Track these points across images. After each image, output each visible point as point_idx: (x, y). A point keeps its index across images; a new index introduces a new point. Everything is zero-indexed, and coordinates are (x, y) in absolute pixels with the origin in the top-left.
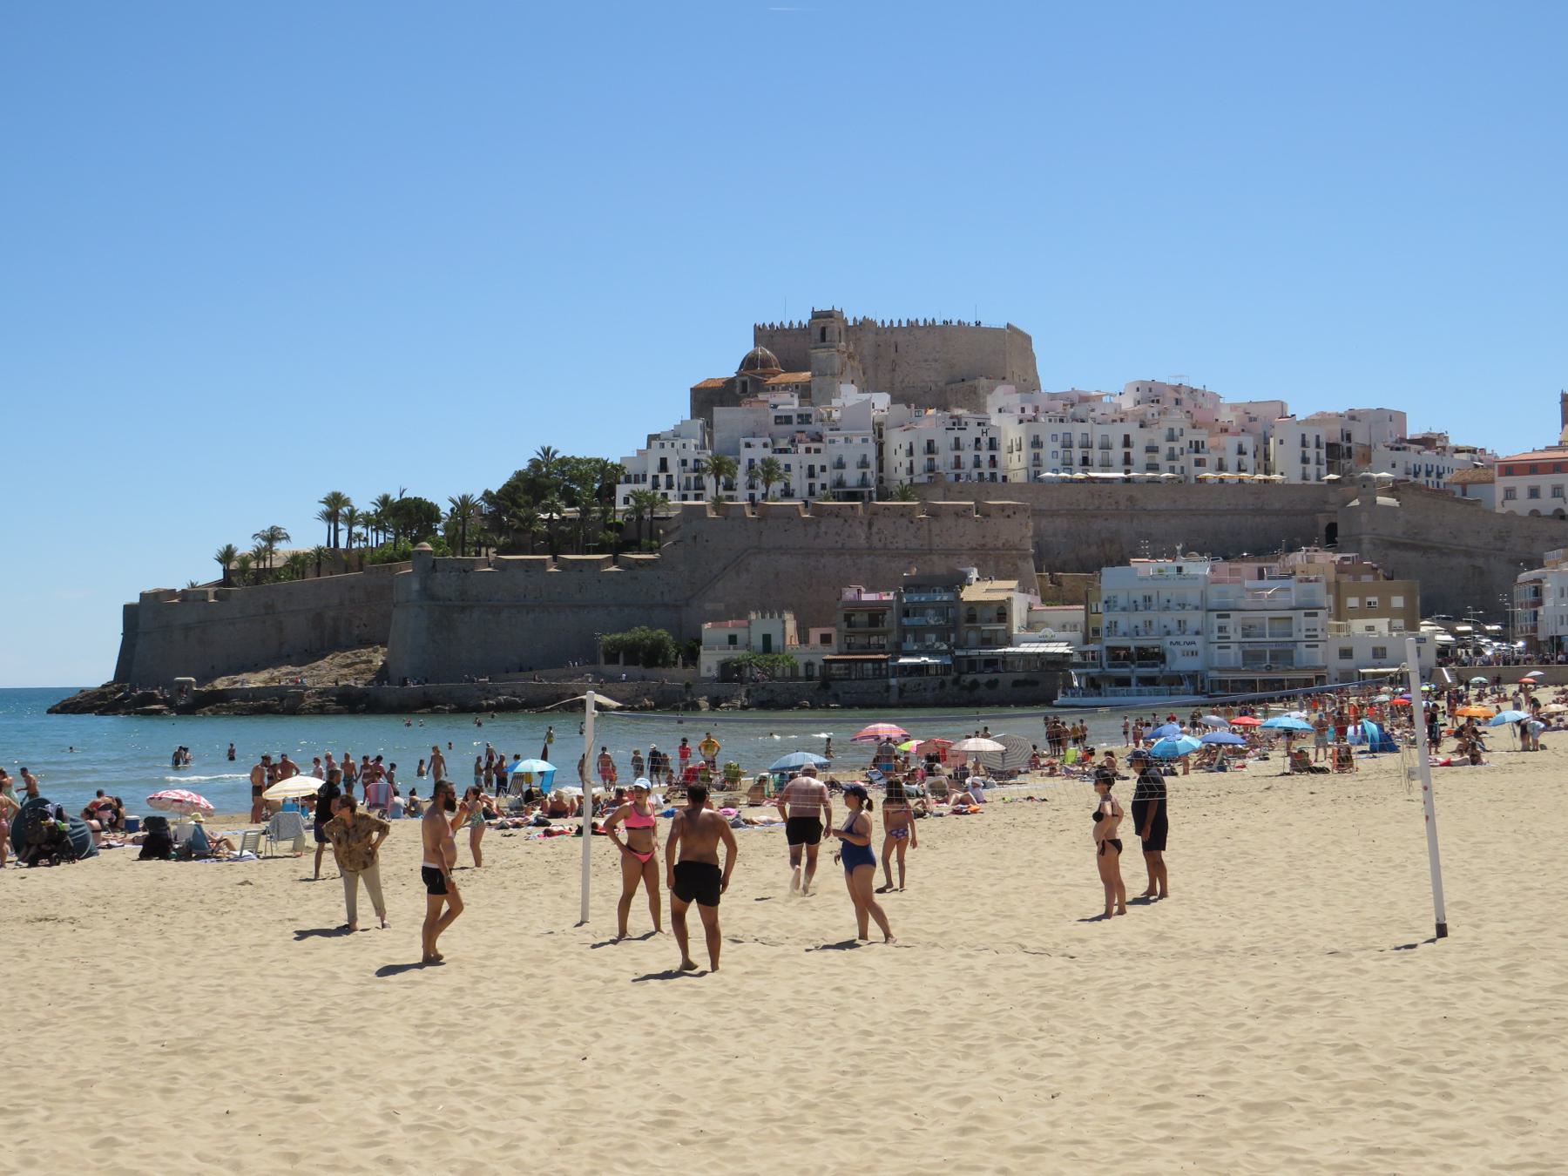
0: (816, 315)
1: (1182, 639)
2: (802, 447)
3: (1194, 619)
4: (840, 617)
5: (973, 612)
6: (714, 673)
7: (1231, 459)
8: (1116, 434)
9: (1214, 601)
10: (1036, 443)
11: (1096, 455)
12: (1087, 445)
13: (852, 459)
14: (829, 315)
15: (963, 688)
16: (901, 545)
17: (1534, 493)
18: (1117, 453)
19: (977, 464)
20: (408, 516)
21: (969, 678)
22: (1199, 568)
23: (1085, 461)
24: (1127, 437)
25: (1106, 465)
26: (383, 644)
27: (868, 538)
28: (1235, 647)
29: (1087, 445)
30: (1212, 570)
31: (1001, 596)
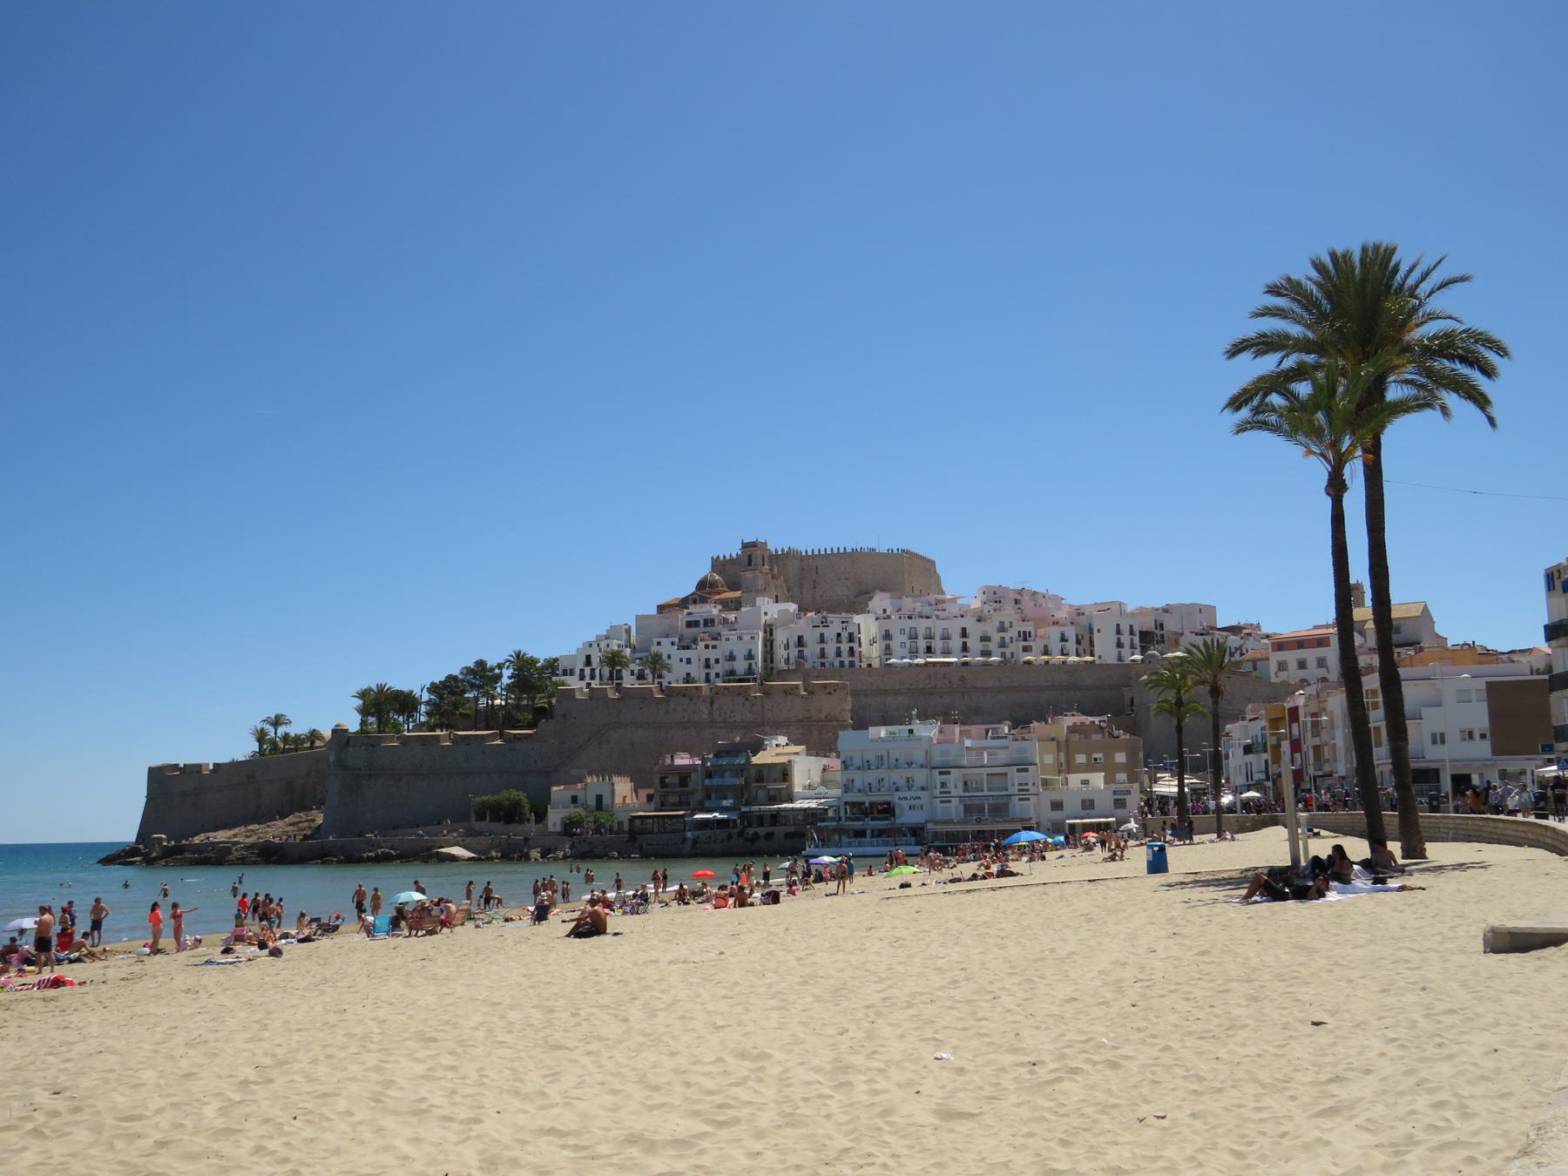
0: (745, 546)
1: (909, 794)
2: (702, 644)
3: (920, 776)
4: (657, 780)
5: (763, 772)
6: (558, 828)
7: (1055, 645)
8: (955, 628)
9: (937, 759)
10: (887, 636)
11: (938, 644)
12: (930, 637)
13: (740, 653)
14: (754, 545)
15: (747, 840)
17: (1302, 665)
18: (956, 643)
19: (839, 654)
20: (383, 704)
21: (751, 831)
22: (928, 731)
23: (929, 650)
24: (964, 630)
25: (947, 653)
26: (320, 804)
27: (710, 713)
28: (955, 801)
29: (930, 637)
30: (941, 732)
31: (783, 759)
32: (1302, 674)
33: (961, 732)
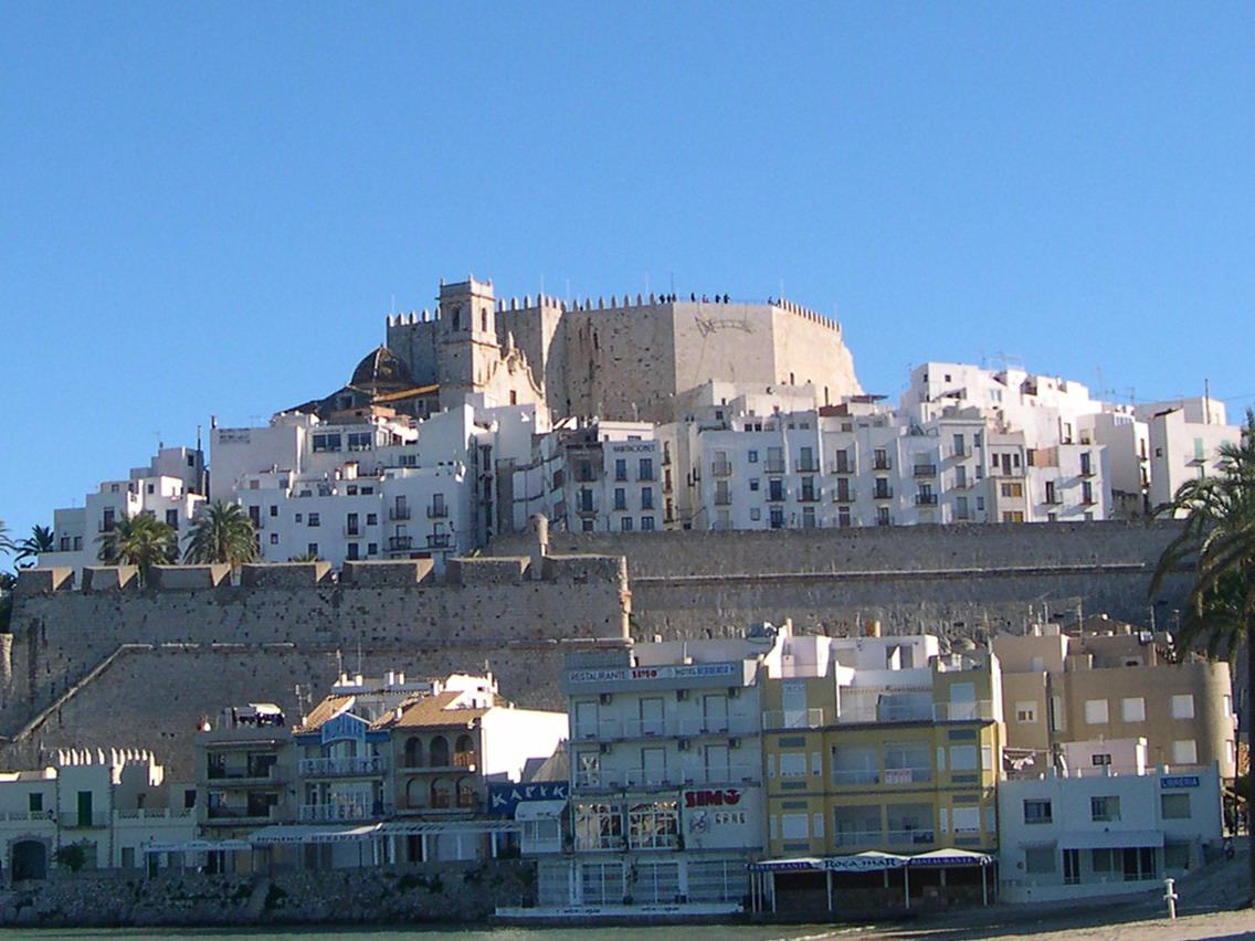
16: (391, 632)
19: (620, 504)
33: (832, 651)
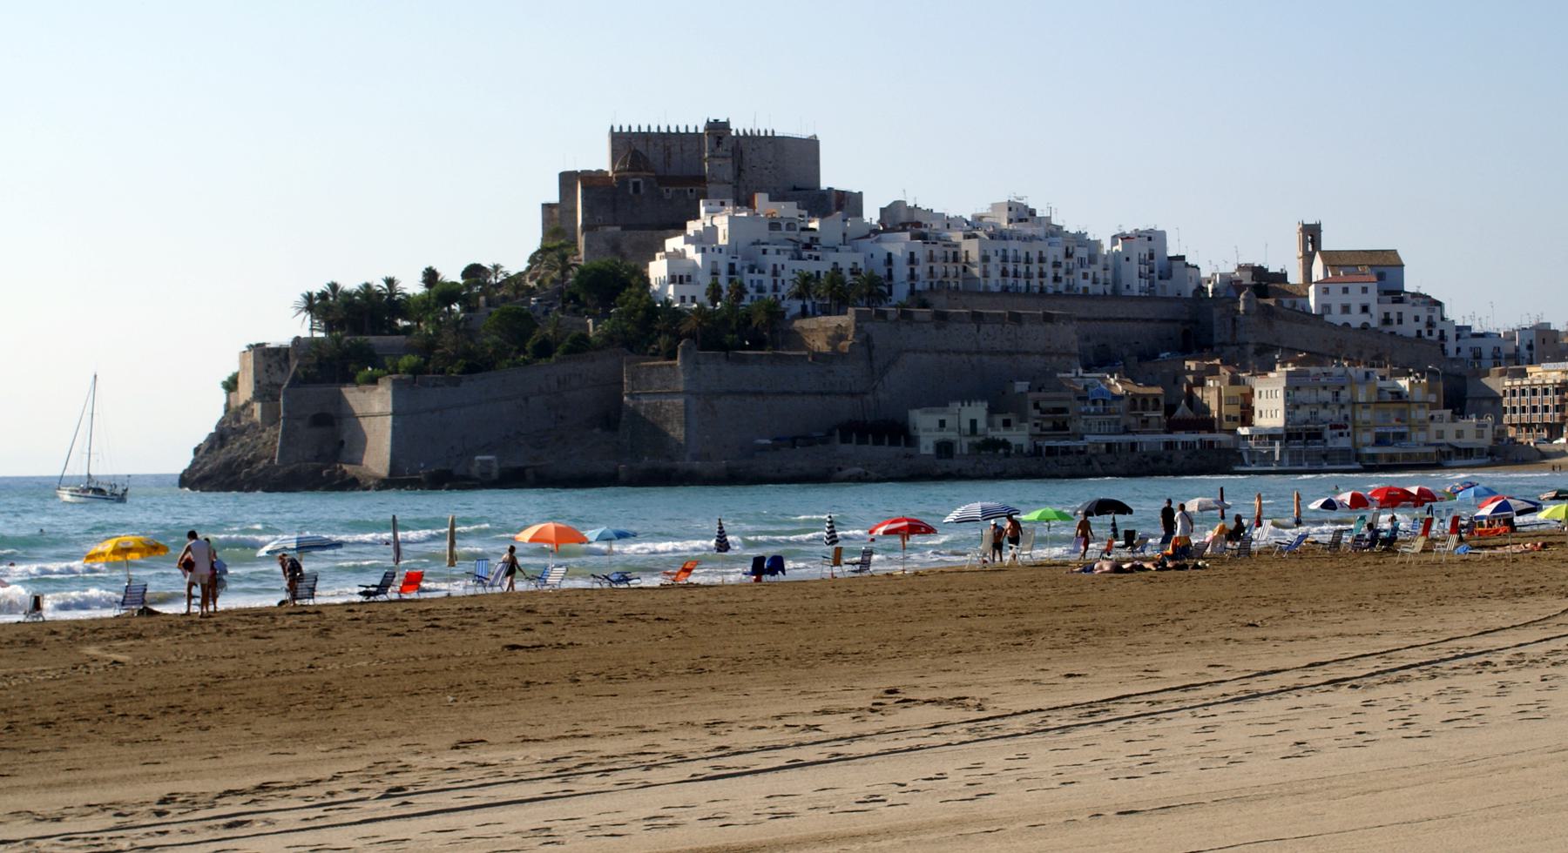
6: (931, 451)
29: (1016, 260)
32: (1365, 318)
